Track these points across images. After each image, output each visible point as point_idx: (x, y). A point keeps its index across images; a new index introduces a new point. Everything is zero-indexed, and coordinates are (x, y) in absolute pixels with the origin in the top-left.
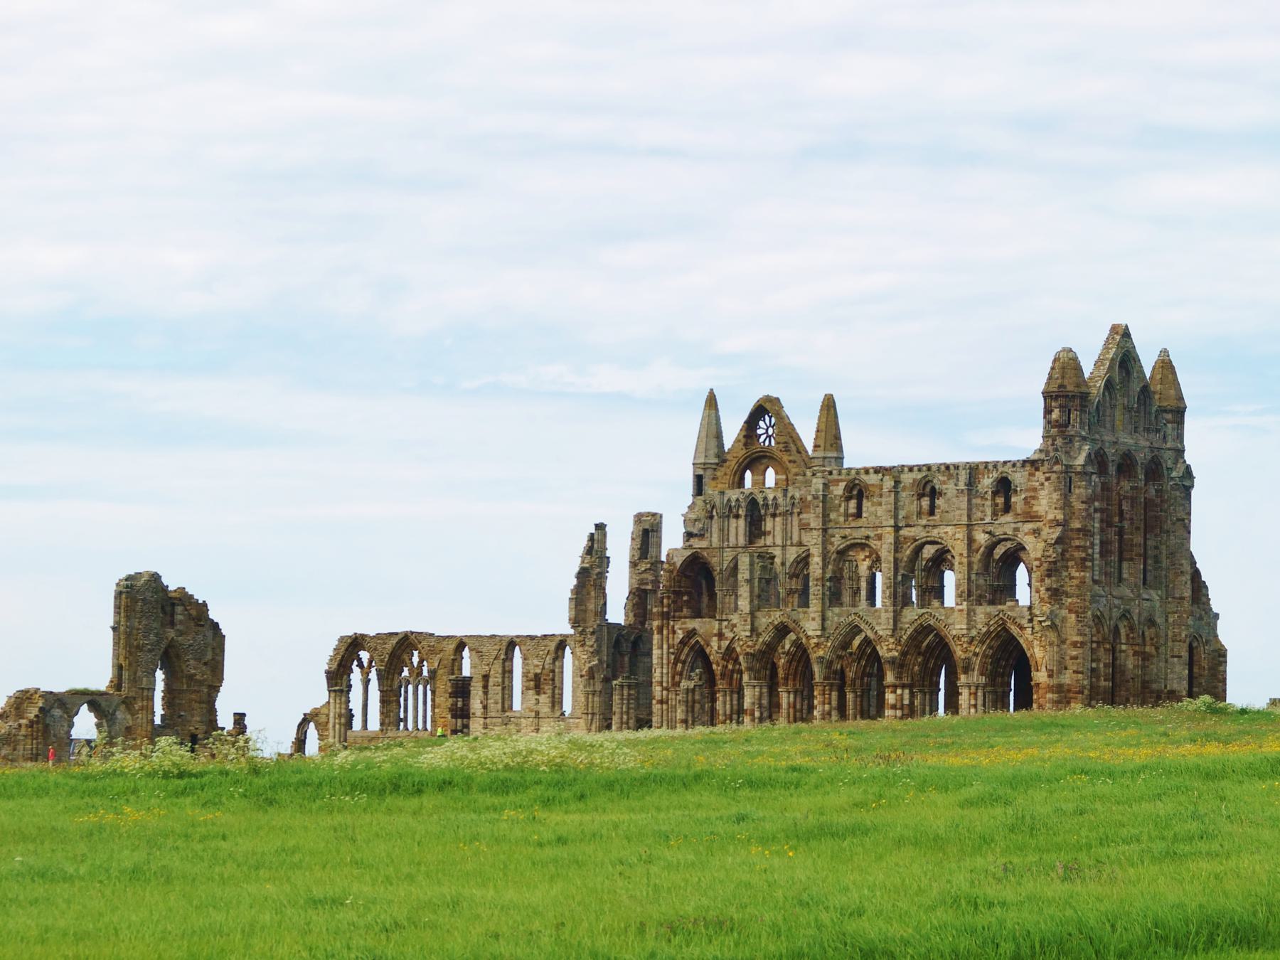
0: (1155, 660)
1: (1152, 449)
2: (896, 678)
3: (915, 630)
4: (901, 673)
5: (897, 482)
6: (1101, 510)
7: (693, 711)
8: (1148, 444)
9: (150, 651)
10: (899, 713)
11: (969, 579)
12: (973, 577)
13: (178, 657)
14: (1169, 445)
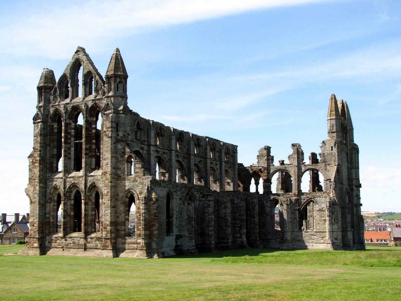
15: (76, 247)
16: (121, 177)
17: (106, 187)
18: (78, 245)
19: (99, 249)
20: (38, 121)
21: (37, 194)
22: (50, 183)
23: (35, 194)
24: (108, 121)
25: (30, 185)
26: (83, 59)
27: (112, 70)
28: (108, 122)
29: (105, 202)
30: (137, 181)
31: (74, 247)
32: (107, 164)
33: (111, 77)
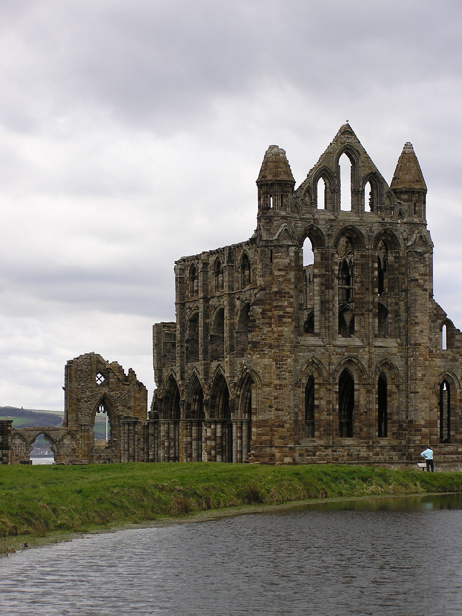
0: (396, 396)
1: (382, 224)
2: (211, 416)
3: (216, 378)
4: (211, 412)
5: (206, 264)
6: (321, 276)
7: (148, 442)
8: (380, 220)
9: (86, 402)
10: (213, 443)
11: (231, 337)
12: (235, 335)
13: (111, 404)
14: (405, 220)
15: (353, 462)
16: (432, 352)
17: (421, 367)
18: (358, 458)
19: (393, 463)
20: (285, 242)
21: (290, 372)
22: (301, 354)
23: (284, 371)
24: (422, 263)
25: (259, 354)
26: (358, 149)
27: (417, 181)
28: (422, 265)
29: (419, 390)
30: (457, 361)
31: (350, 462)
32: (422, 332)
33: (418, 192)
